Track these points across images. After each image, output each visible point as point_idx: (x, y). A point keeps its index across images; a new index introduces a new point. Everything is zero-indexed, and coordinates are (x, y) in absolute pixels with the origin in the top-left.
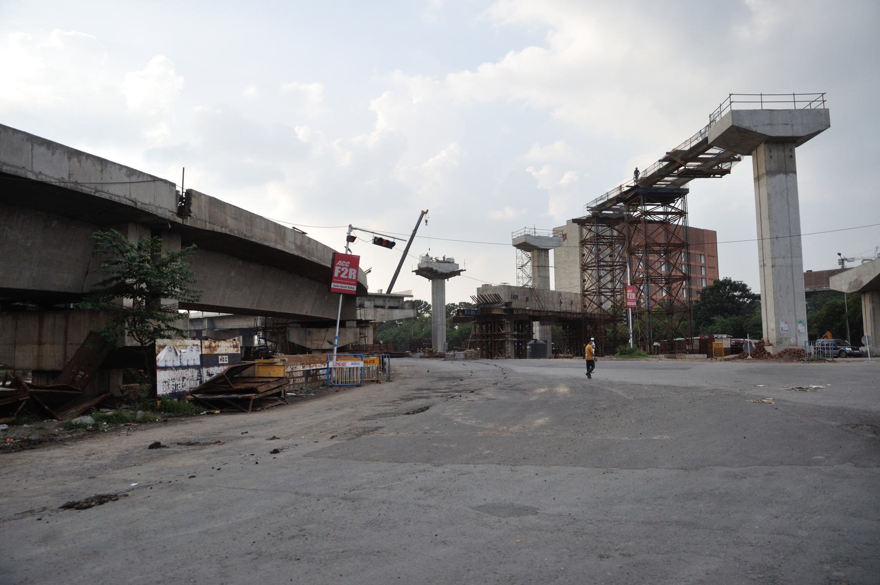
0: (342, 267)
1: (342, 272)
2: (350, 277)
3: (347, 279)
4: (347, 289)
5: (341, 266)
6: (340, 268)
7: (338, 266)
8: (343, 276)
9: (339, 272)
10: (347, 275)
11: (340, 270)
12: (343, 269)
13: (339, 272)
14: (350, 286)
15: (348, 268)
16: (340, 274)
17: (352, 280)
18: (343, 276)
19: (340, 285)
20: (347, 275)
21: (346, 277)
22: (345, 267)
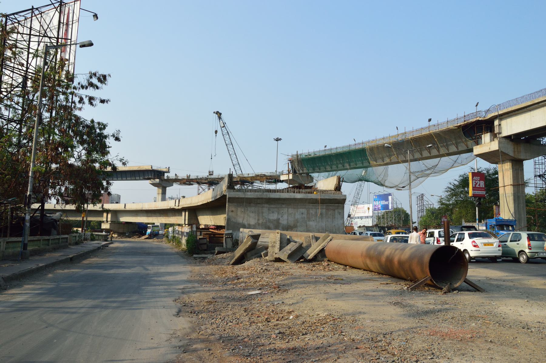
0: (476, 180)
1: (477, 184)
2: (481, 186)
3: (480, 188)
4: (481, 194)
5: (475, 180)
6: (475, 181)
7: (474, 180)
8: (477, 186)
9: (475, 184)
10: (479, 185)
11: (475, 182)
12: (477, 182)
13: (475, 184)
14: (482, 192)
15: (479, 181)
16: (475, 185)
17: (482, 188)
18: (477, 186)
19: (476, 191)
20: (479, 185)
21: (479, 186)
22: (477, 180)
